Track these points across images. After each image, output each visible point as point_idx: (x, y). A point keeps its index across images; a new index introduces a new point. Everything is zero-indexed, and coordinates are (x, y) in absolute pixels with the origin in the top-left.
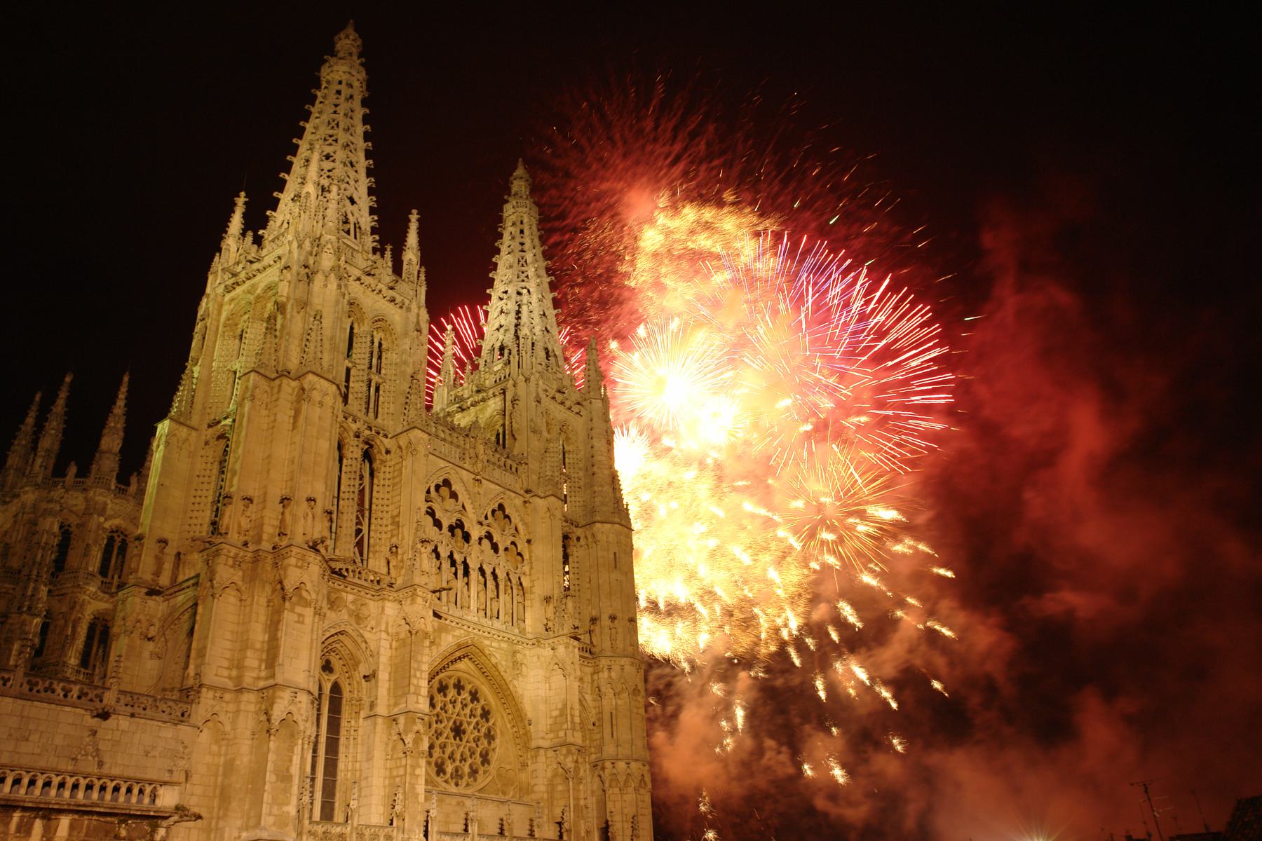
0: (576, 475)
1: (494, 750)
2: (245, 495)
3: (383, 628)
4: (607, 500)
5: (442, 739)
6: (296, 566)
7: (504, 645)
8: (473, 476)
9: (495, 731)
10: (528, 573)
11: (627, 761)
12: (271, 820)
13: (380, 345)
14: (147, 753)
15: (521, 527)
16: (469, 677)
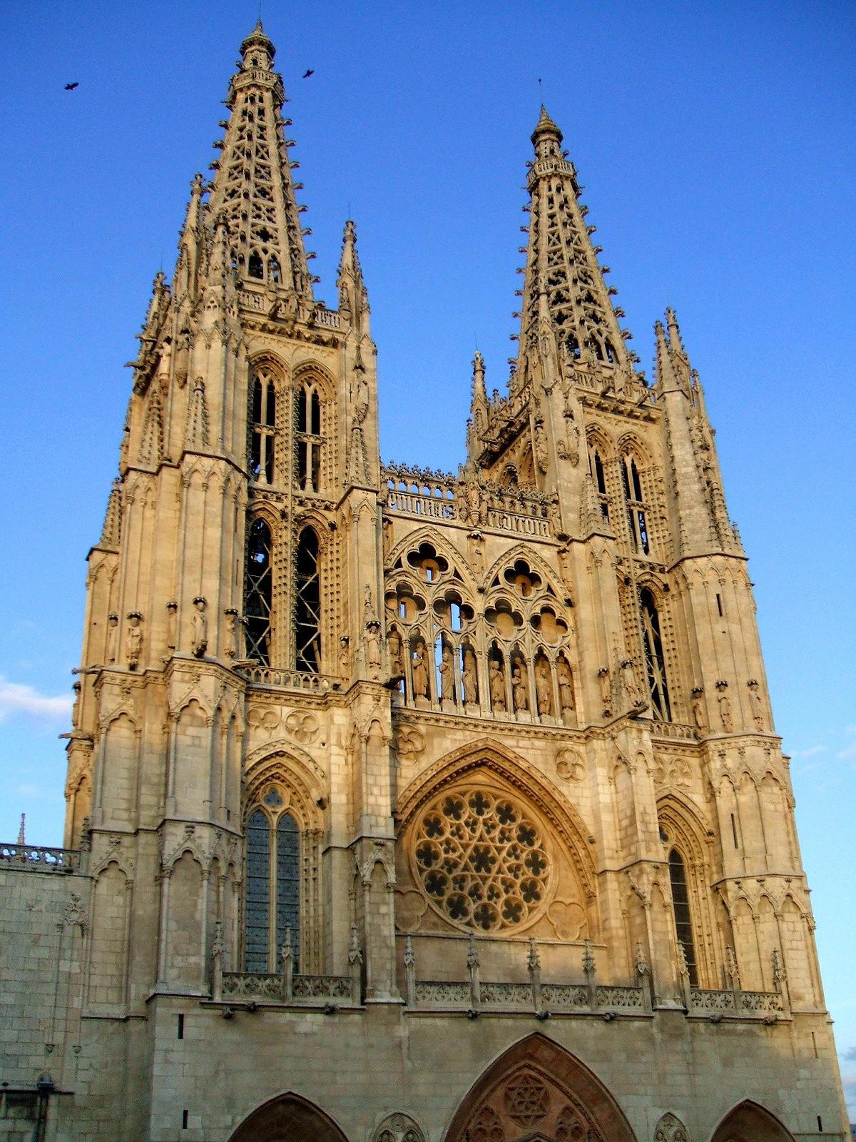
0: (656, 502)
1: (544, 880)
2: (133, 611)
3: (333, 740)
4: (700, 524)
5: (457, 872)
6: (183, 681)
7: (540, 744)
8: (468, 533)
9: (544, 856)
10: (573, 643)
11: (759, 878)
12: (173, 973)
13: (315, 396)
14: (30, 908)
15: (556, 586)
16: (494, 791)
